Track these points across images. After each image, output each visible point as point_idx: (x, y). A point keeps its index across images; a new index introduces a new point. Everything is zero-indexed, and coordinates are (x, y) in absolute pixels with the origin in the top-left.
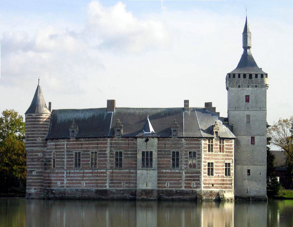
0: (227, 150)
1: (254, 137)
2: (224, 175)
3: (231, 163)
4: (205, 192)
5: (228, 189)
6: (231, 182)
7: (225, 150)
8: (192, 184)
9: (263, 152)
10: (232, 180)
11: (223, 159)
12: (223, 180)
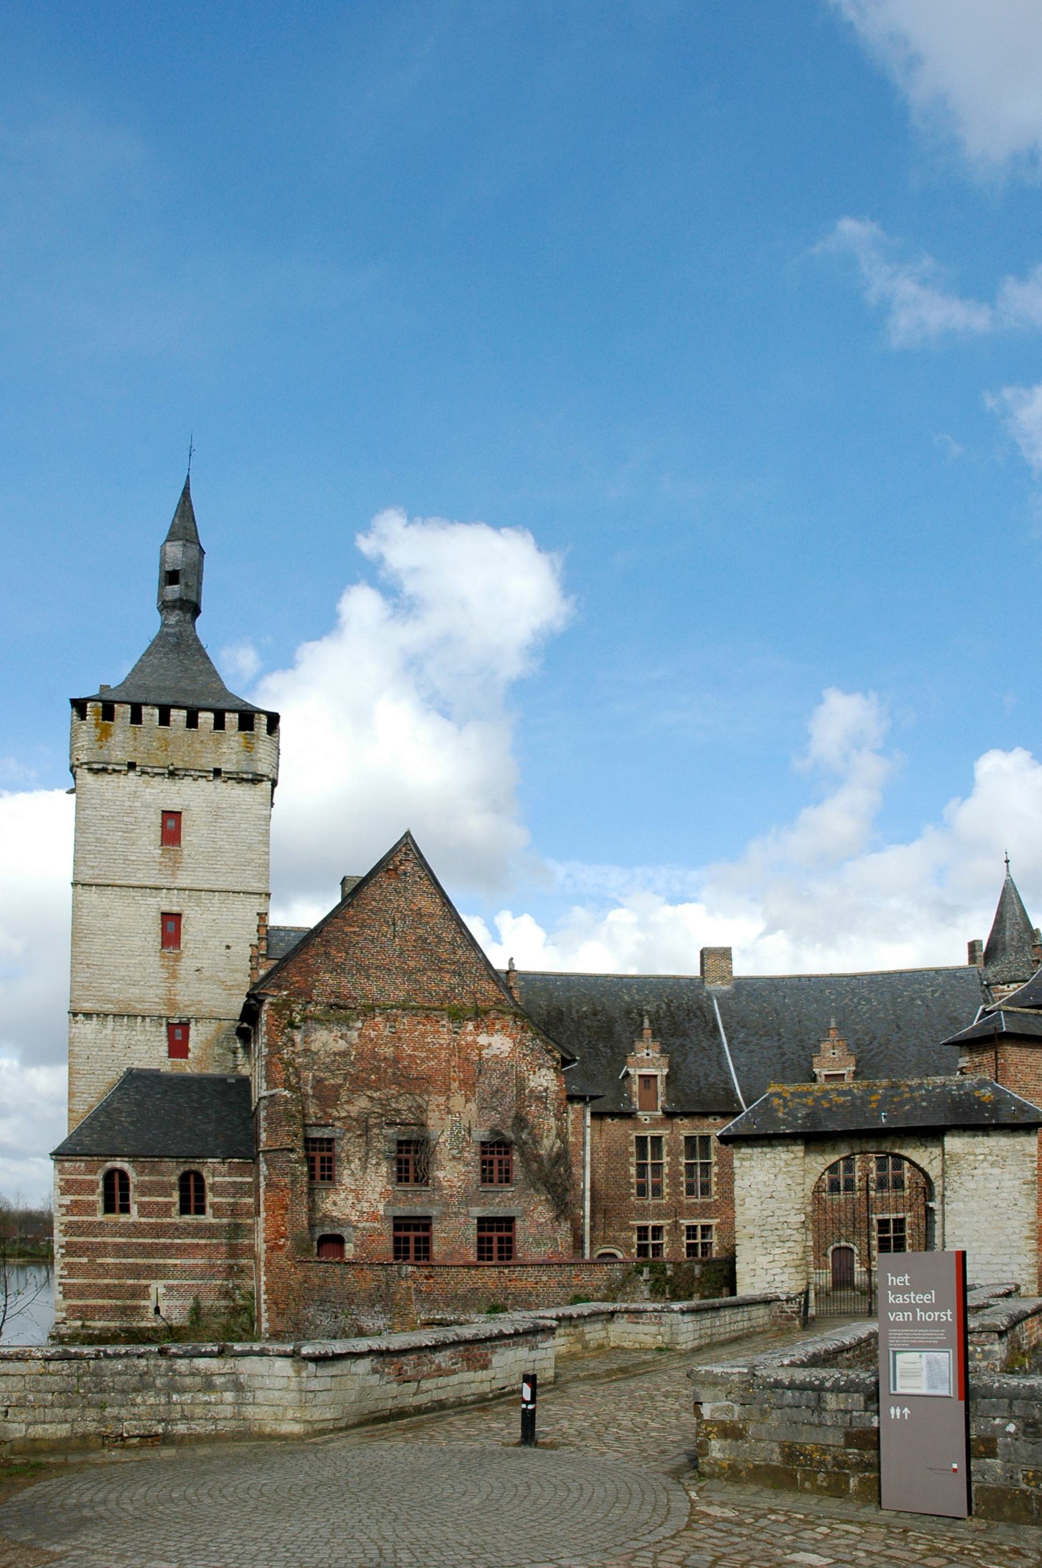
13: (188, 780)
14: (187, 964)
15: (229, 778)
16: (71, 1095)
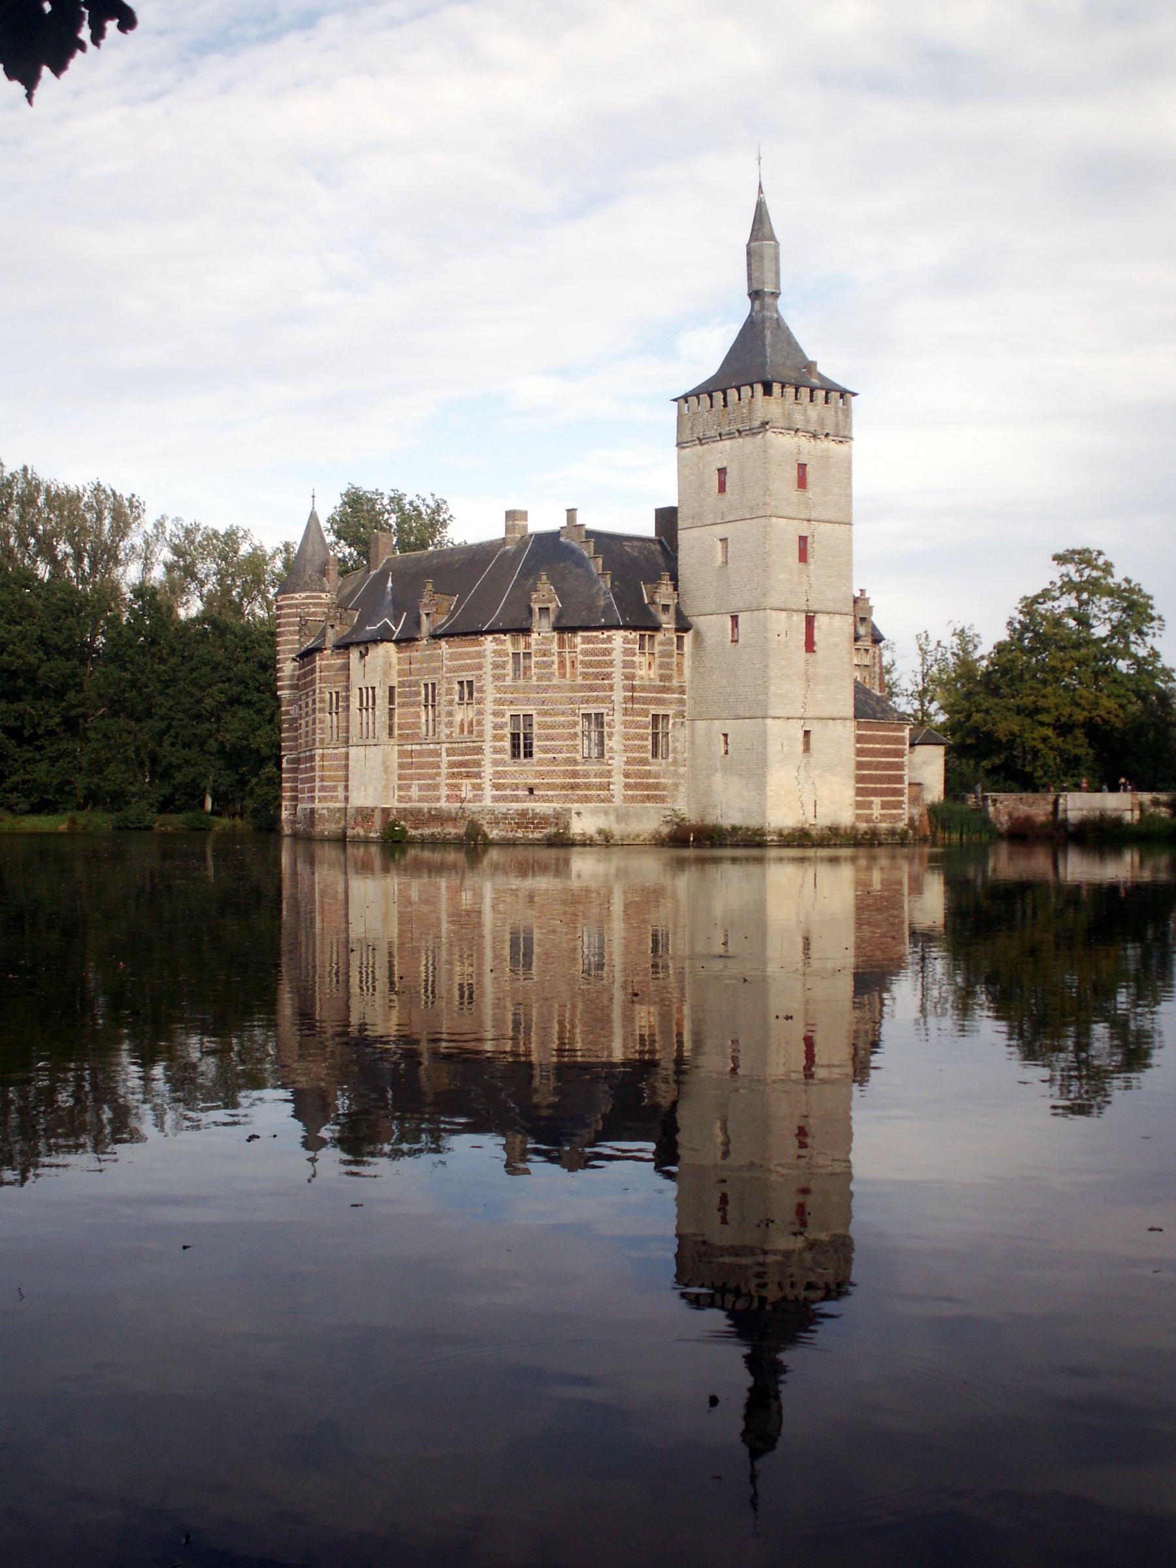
0: (591, 670)
1: (737, 616)
2: (649, 755)
3: (608, 715)
4: (500, 816)
5: (592, 805)
6: (607, 780)
7: (580, 669)
8: (463, 788)
9: (760, 669)
10: (609, 772)
11: (572, 701)
12: (575, 774)
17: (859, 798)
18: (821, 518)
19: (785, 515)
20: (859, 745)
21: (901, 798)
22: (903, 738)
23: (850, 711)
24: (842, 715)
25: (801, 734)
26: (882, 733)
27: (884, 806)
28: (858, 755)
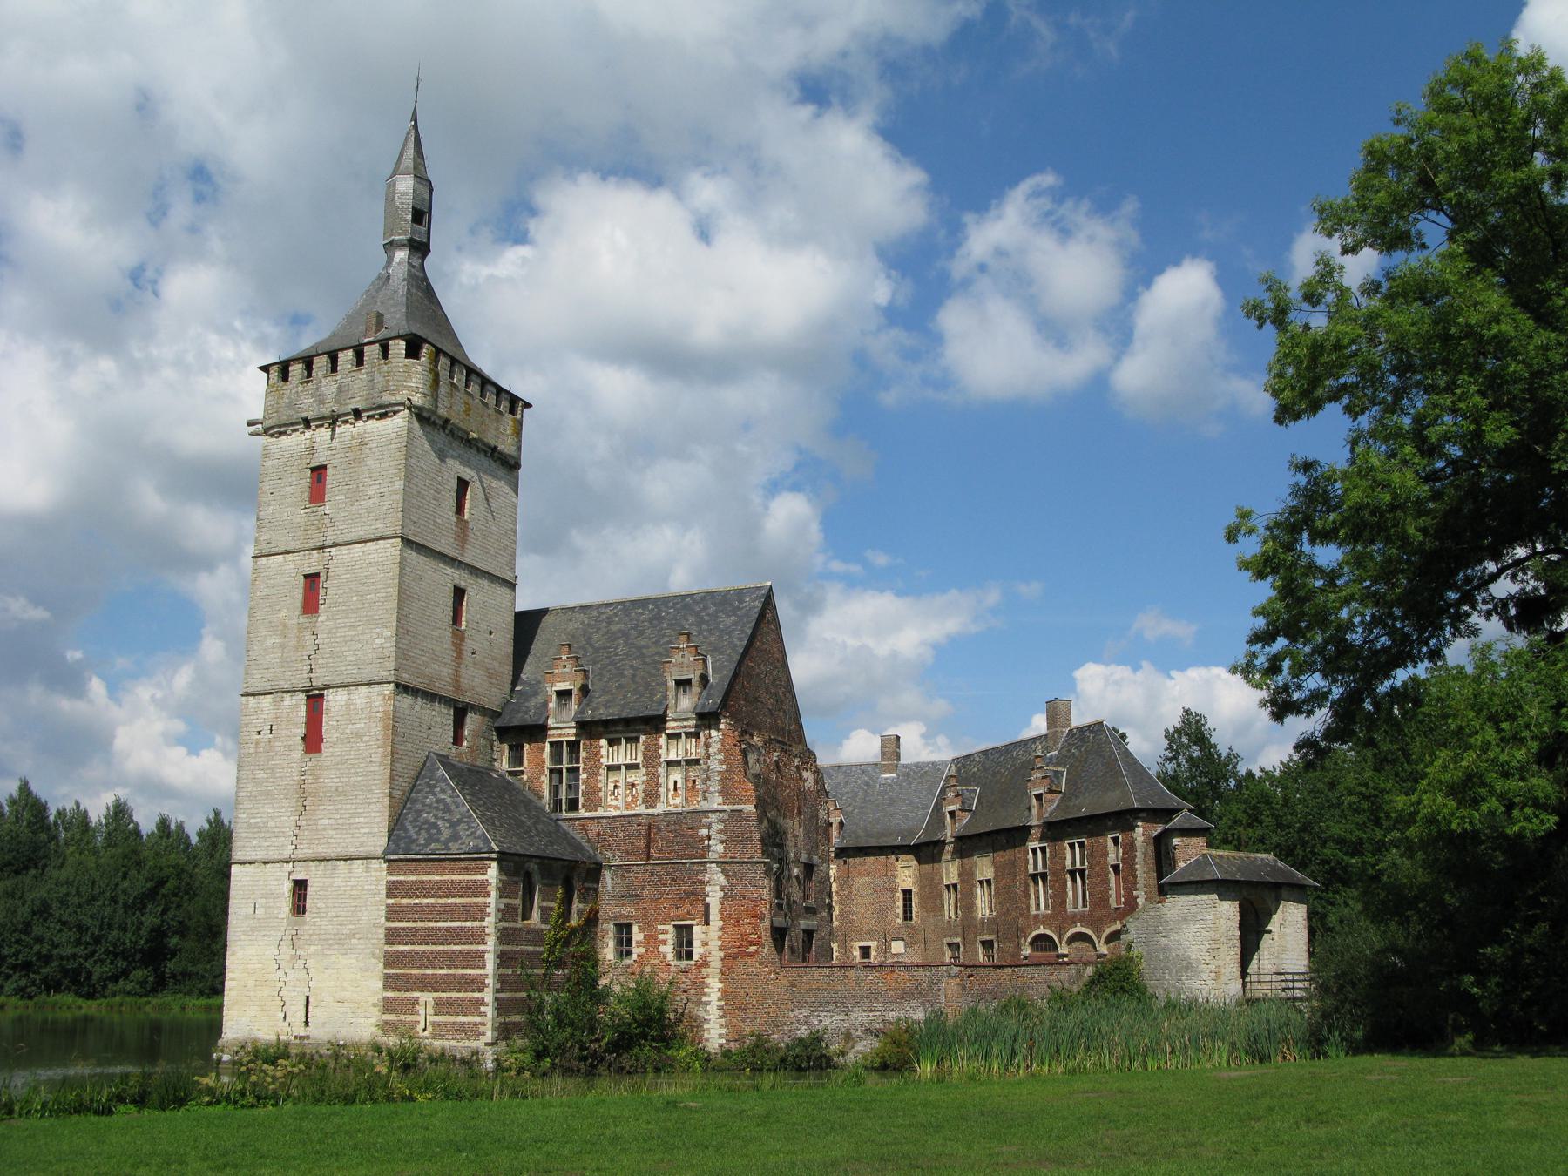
13: (474, 451)
14: (469, 645)
15: (500, 459)
16: (392, 779)
17: (390, 994)
18: (341, 540)
19: (282, 549)
20: (391, 901)
21: (477, 995)
22: (484, 884)
23: (379, 843)
24: (363, 851)
25: (287, 886)
26: (437, 878)
27: (440, 1007)
28: (388, 919)
